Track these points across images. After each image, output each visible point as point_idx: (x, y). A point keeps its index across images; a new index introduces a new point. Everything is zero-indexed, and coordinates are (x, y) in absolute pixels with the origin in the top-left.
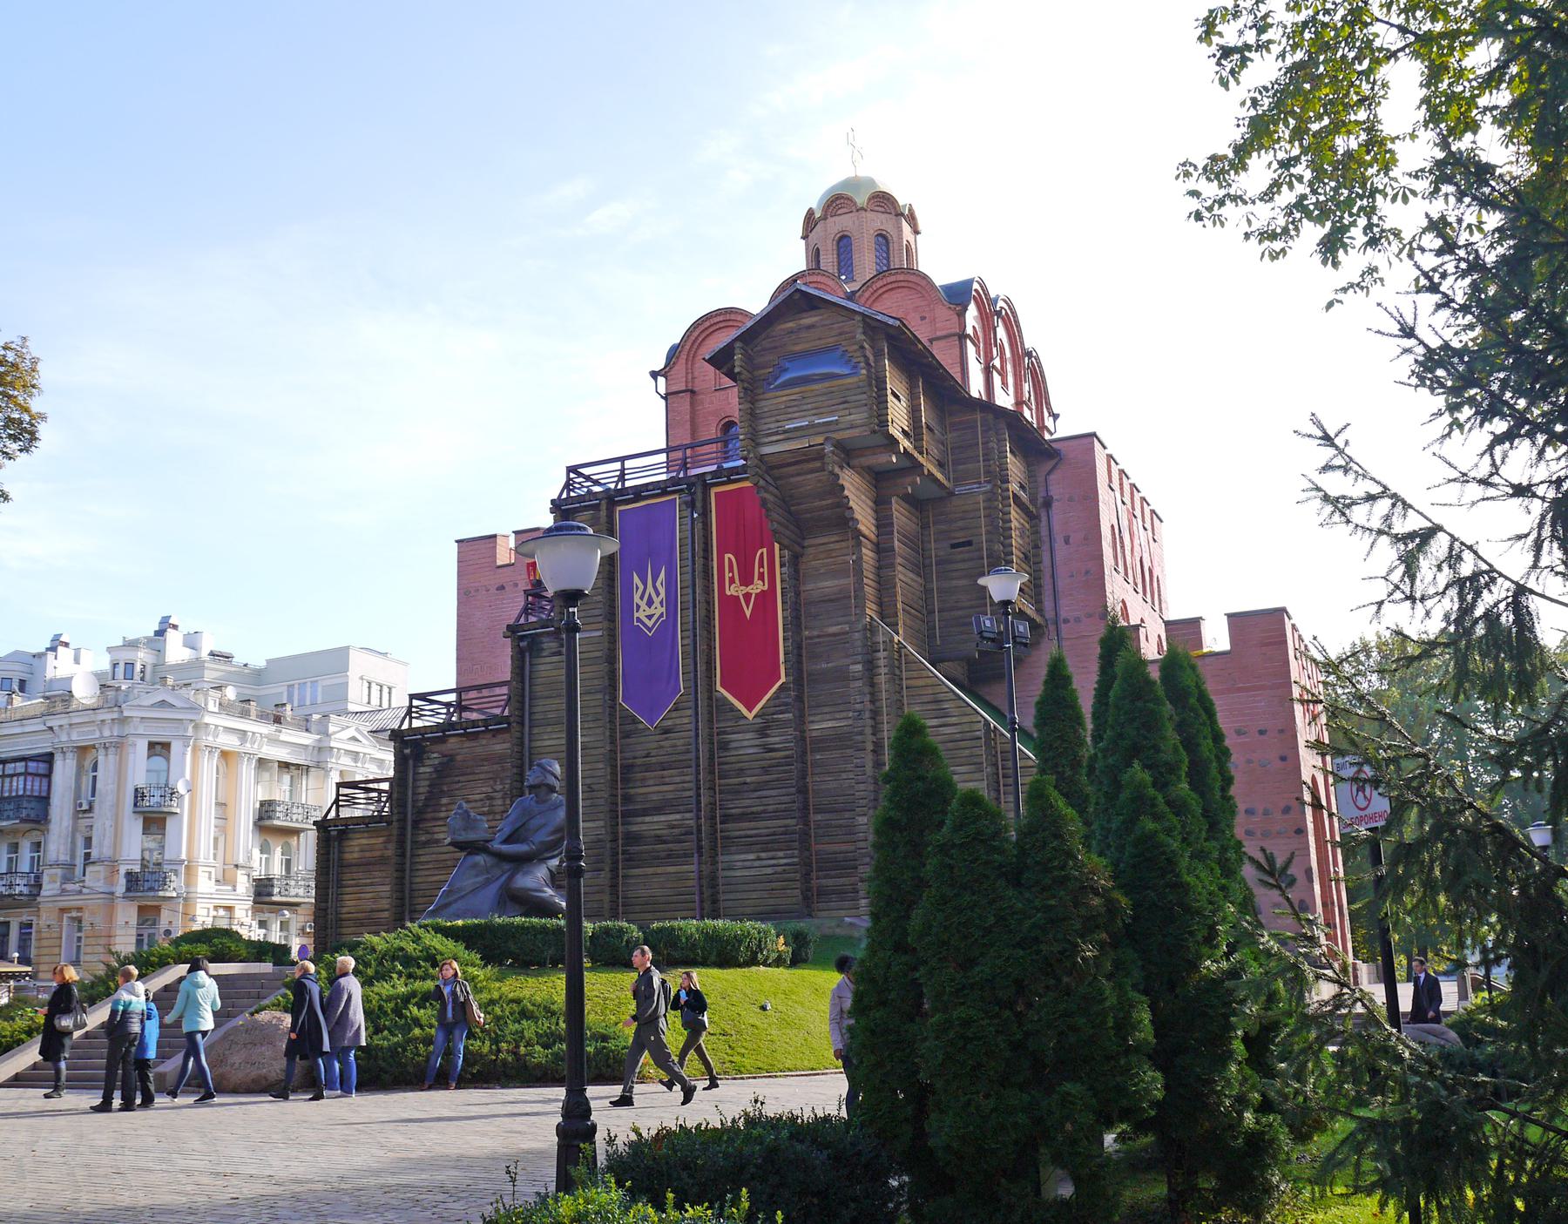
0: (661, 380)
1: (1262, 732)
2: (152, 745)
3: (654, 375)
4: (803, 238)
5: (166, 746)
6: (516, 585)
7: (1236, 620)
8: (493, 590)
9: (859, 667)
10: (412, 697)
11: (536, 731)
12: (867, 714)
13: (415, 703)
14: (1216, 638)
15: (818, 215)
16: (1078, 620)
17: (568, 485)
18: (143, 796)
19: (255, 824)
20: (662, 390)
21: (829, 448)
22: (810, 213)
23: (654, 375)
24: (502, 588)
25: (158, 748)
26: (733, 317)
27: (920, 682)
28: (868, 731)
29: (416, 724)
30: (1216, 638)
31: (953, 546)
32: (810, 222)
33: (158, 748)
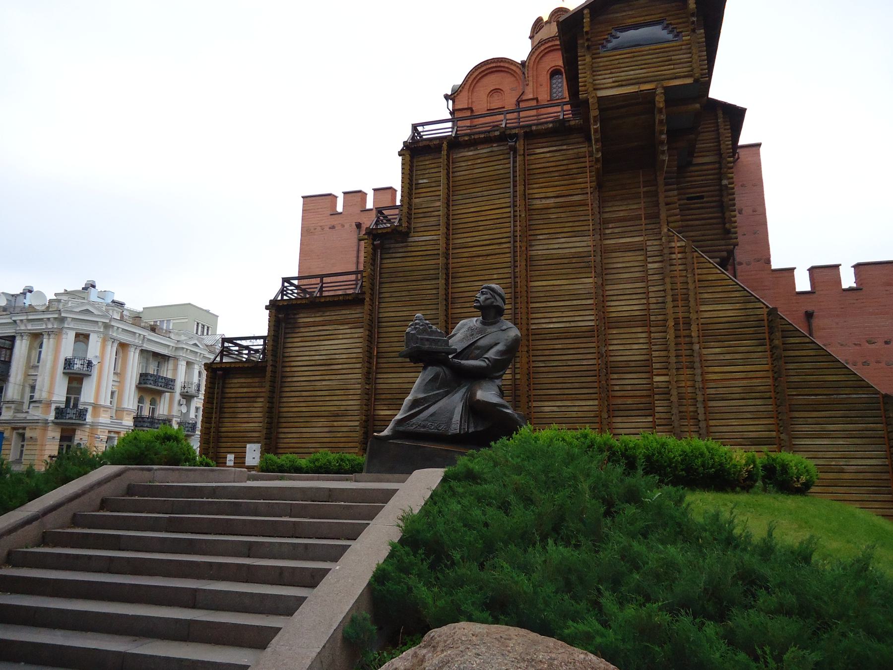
0: (450, 102)
1: (886, 343)
2: (78, 335)
3: (447, 97)
4: (530, 38)
5: (86, 337)
6: (343, 226)
7: (858, 267)
8: (327, 229)
9: (656, 265)
10: (285, 280)
11: (383, 305)
12: (669, 299)
13: (286, 284)
14: (848, 280)
15: (546, 18)
16: (748, 264)
17: (413, 137)
18: (70, 364)
19: (137, 386)
20: (451, 107)
21: (659, 91)
22: (539, 20)
23: (447, 97)
24: (333, 227)
25: (81, 337)
26: (502, 64)
27: (710, 277)
28: (670, 311)
29: (285, 298)
30: (848, 280)
31: (688, 199)
32: (538, 25)
33: (81, 337)
